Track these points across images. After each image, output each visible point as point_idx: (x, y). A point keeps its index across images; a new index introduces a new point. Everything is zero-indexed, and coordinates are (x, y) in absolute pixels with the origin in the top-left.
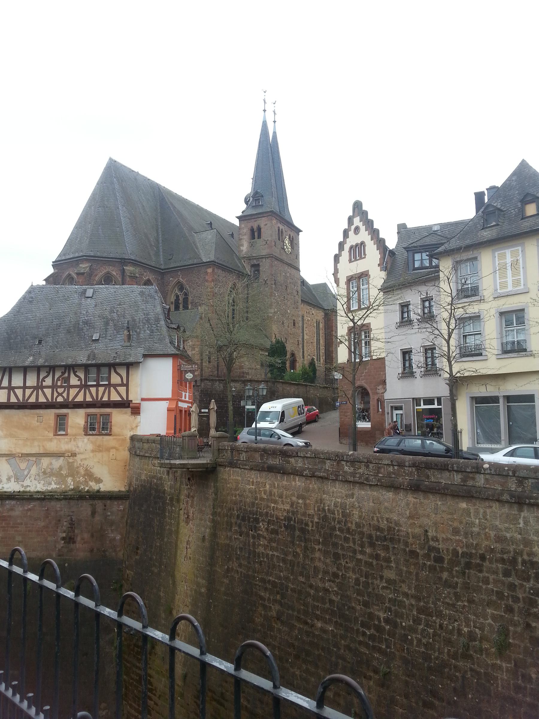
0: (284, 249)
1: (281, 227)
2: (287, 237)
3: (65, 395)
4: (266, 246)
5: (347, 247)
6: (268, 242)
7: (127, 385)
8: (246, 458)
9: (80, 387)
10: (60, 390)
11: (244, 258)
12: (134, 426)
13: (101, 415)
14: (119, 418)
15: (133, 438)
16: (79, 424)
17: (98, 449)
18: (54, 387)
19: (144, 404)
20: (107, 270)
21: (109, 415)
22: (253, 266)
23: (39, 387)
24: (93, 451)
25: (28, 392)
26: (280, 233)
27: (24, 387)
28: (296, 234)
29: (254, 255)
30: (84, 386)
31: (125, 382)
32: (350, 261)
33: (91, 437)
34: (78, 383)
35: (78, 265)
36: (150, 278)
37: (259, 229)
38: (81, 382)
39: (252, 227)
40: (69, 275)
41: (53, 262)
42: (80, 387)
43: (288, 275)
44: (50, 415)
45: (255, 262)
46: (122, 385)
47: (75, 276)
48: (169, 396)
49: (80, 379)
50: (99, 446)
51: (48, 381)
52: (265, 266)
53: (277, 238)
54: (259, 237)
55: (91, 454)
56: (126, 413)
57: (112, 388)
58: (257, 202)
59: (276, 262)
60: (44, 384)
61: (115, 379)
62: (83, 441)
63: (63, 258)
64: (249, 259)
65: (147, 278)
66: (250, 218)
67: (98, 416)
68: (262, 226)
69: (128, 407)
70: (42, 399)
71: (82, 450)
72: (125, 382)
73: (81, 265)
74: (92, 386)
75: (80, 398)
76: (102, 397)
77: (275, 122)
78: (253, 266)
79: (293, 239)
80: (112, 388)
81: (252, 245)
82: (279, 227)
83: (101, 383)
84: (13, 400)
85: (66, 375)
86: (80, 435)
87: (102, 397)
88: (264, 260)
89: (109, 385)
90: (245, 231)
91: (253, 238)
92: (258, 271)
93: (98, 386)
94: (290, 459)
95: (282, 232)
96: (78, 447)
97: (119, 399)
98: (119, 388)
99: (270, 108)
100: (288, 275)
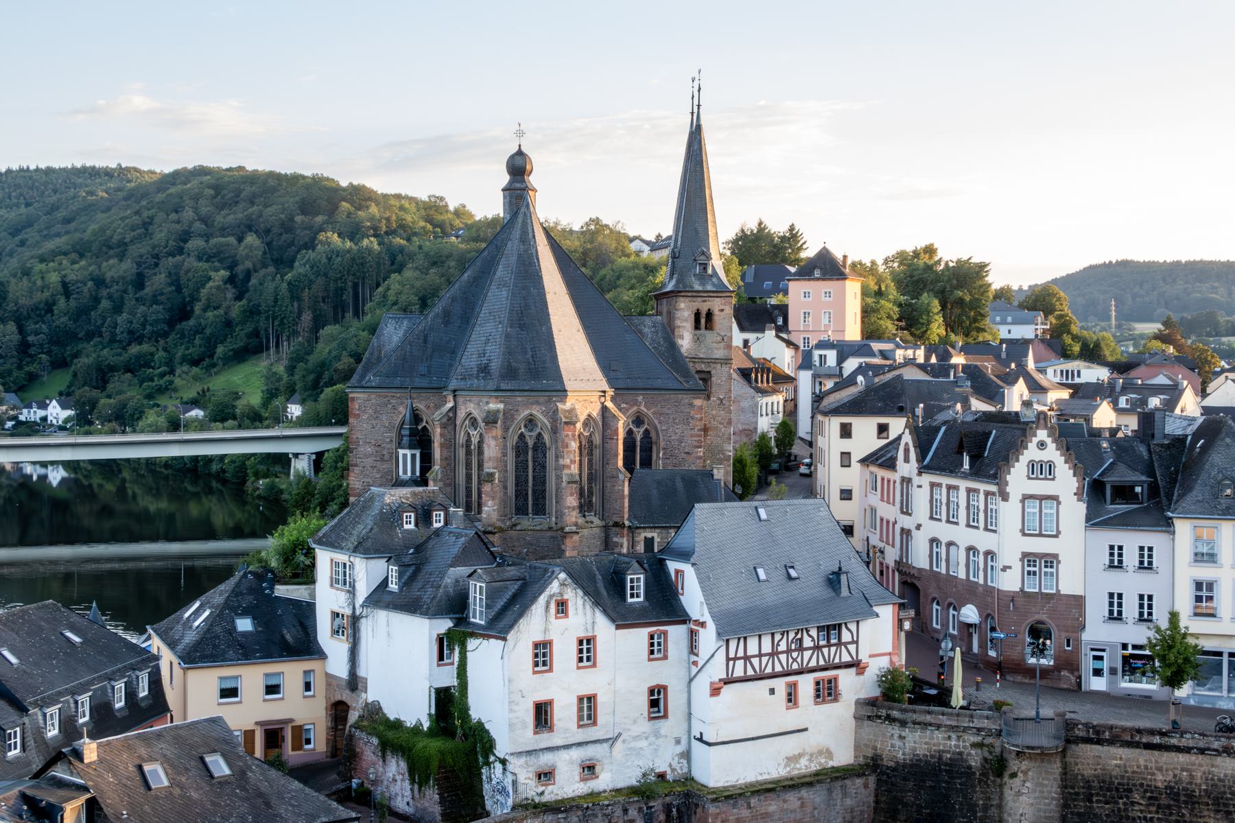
3: (799, 660)
4: (722, 345)
7: (857, 642)
10: (795, 655)
18: (788, 651)
21: (836, 679)
23: (774, 654)
25: (764, 659)
27: (760, 655)
34: (811, 644)
37: (709, 315)
44: (780, 684)
45: (703, 367)
46: (853, 642)
48: (890, 649)
51: (783, 646)
60: (780, 649)
61: (846, 636)
68: (716, 312)
70: (778, 668)
75: (813, 663)
81: (697, 340)
84: (750, 672)
85: (799, 636)
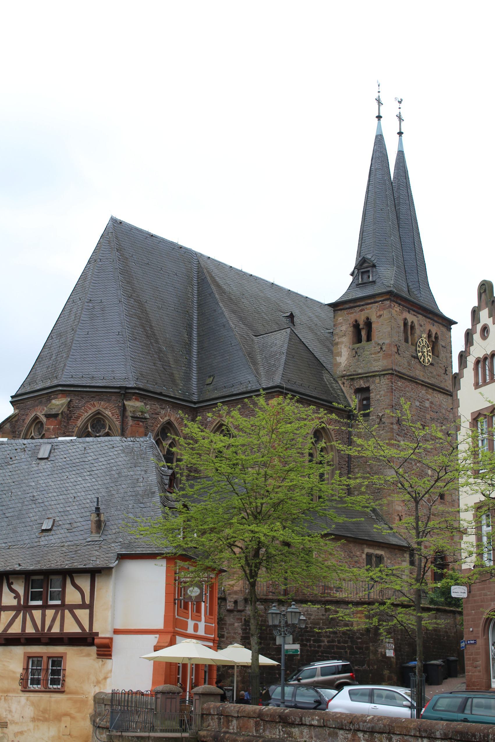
0: (416, 358)
1: (411, 318)
2: (425, 336)
5: (471, 361)
6: (384, 348)
7: (90, 607)
8: (237, 728)
9: (17, 609)
11: (343, 376)
12: (101, 677)
13: (49, 658)
14: (78, 662)
15: (99, 700)
16: (14, 672)
17: (43, 717)
19: (119, 641)
20: (96, 409)
22: (358, 391)
24: (34, 720)
26: (408, 329)
28: (444, 329)
29: (360, 371)
30: (23, 608)
31: (87, 601)
32: (477, 386)
33: (32, 695)
34: (14, 603)
35: (49, 400)
36: (172, 419)
37: (369, 324)
38: (19, 602)
39: (356, 321)
40: (36, 418)
41: (12, 397)
42: (17, 609)
43: (427, 404)
45: (362, 384)
46: (83, 606)
47: (44, 419)
48: (159, 624)
49: (17, 596)
50: (44, 711)
52: (380, 389)
53: (402, 337)
54: (369, 339)
55: (31, 725)
56: (88, 655)
57: (67, 612)
58: (365, 277)
59: (400, 384)
61: (72, 596)
62: (19, 702)
63: (28, 389)
64: (352, 378)
65: (167, 418)
66: (352, 305)
67: (45, 659)
68: (373, 319)
69: (92, 644)
71: (16, 717)
72: (87, 601)
73: (54, 401)
74: (36, 607)
75: (16, 629)
76: (50, 628)
77: (400, 133)
78: (358, 391)
79: (436, 338)
80: (67, 612)
81: (356, 354)
82: (405, 319)
83: (51, 603)
86: (14, 691)
87: (50, 628)
88: (377, 380)
89: (63, 606)
90: (344, 328)
91: (359, 340)
92: (368, 399)
93: (45, 607)
94: (293, 730)
95: (412, 327)
96: (10, 711)
97: (77, 630)
98: (77, 612)
99: (389, 112)
100: (427, 404)
